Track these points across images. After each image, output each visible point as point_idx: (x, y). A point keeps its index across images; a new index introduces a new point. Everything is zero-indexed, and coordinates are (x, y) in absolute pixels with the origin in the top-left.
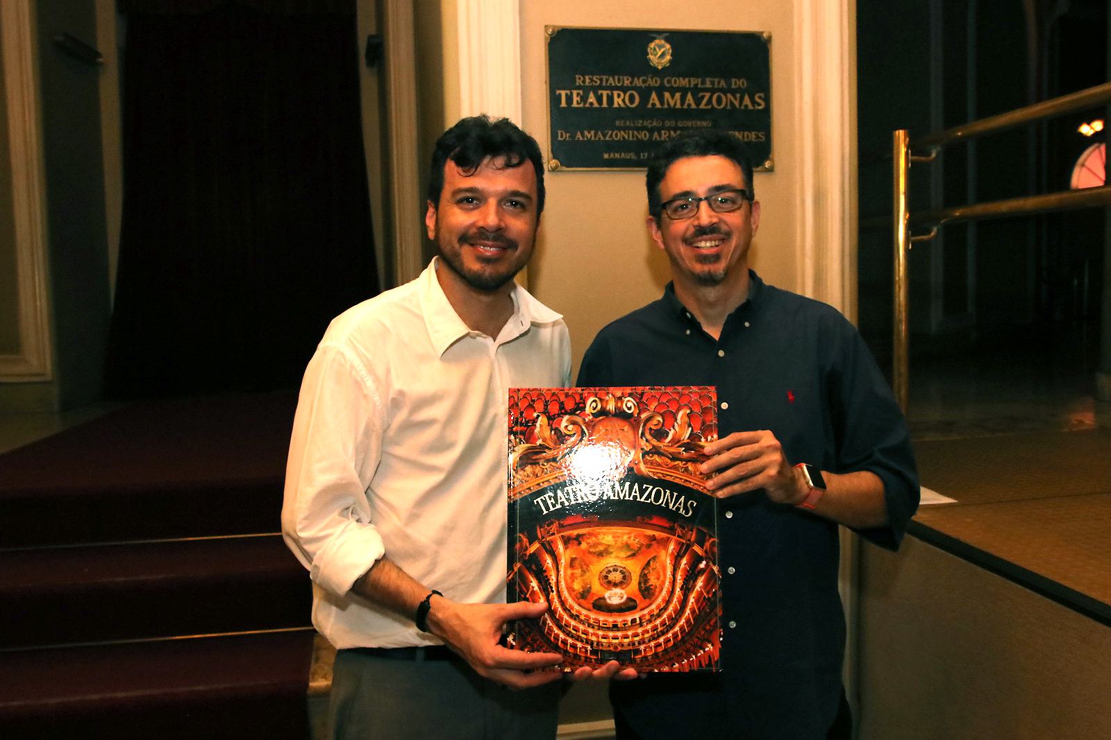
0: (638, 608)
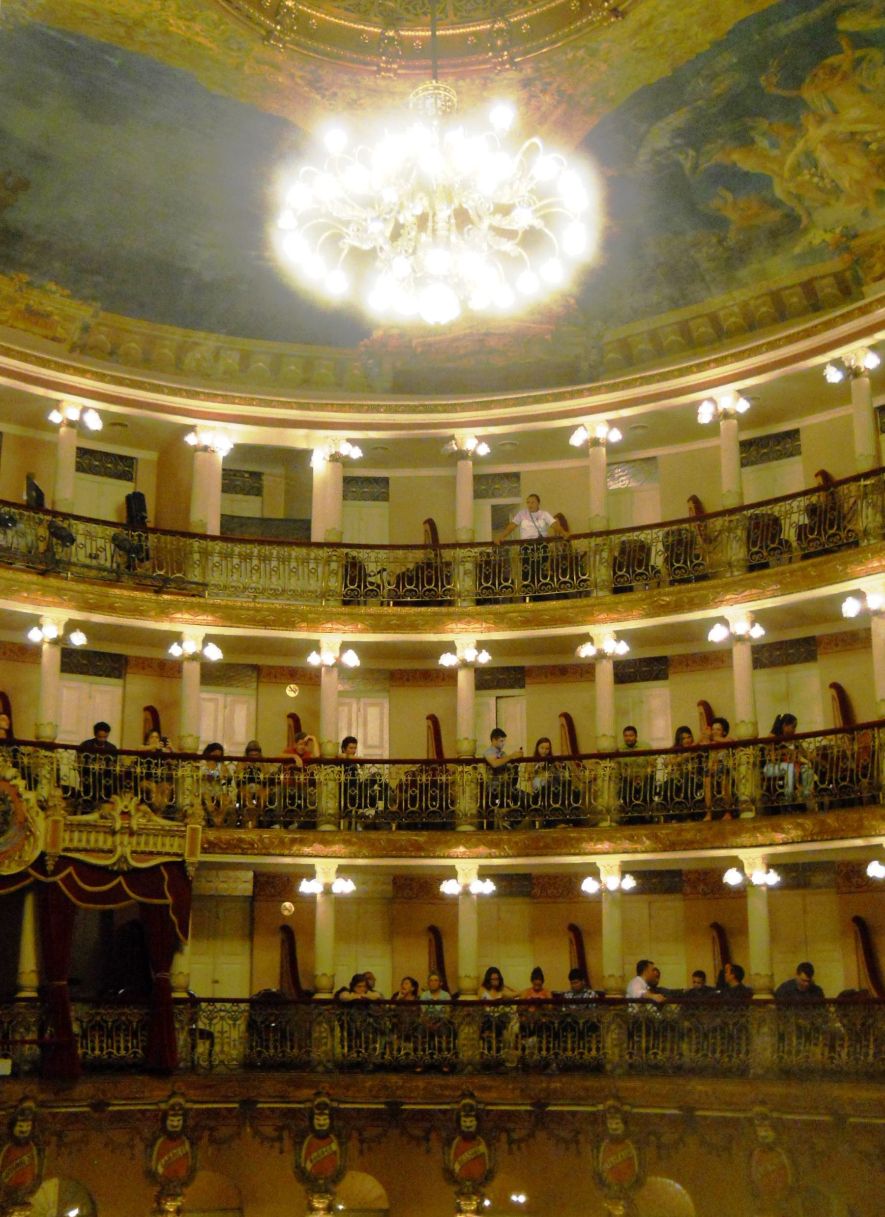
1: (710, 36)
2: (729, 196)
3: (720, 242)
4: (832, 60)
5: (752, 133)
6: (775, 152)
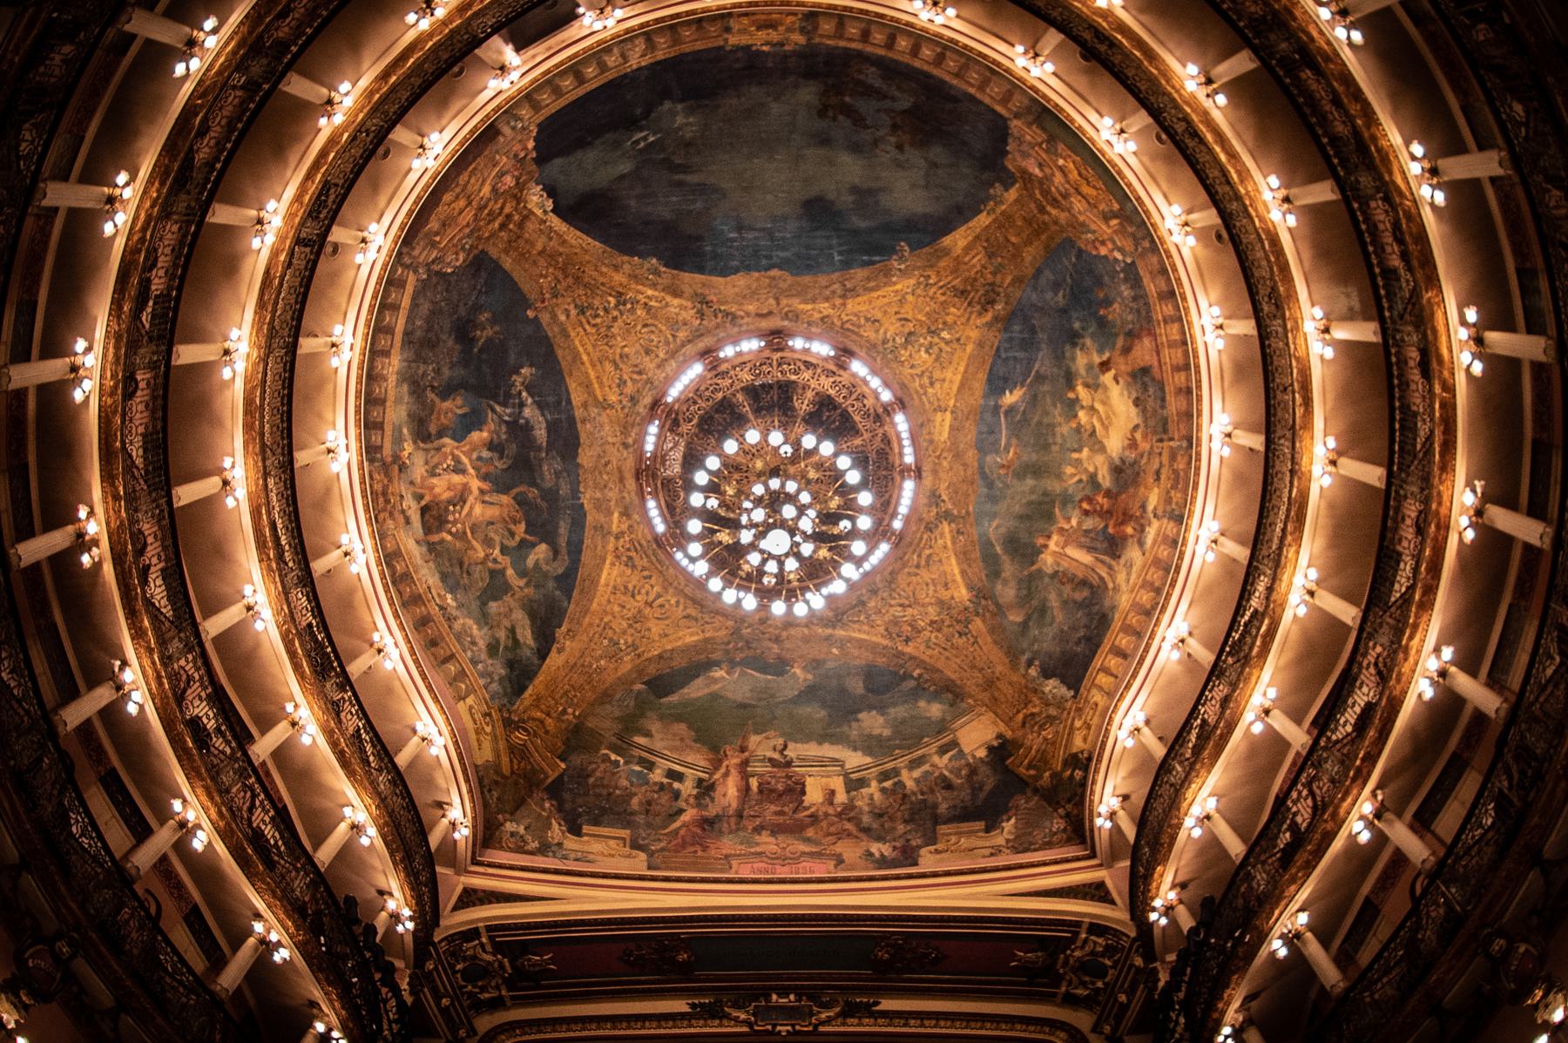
0: (521, 140)
2: (459, 412)
3: (433, 387)
4: (523, 526)
5: (496, 455)
6: (474, 456)
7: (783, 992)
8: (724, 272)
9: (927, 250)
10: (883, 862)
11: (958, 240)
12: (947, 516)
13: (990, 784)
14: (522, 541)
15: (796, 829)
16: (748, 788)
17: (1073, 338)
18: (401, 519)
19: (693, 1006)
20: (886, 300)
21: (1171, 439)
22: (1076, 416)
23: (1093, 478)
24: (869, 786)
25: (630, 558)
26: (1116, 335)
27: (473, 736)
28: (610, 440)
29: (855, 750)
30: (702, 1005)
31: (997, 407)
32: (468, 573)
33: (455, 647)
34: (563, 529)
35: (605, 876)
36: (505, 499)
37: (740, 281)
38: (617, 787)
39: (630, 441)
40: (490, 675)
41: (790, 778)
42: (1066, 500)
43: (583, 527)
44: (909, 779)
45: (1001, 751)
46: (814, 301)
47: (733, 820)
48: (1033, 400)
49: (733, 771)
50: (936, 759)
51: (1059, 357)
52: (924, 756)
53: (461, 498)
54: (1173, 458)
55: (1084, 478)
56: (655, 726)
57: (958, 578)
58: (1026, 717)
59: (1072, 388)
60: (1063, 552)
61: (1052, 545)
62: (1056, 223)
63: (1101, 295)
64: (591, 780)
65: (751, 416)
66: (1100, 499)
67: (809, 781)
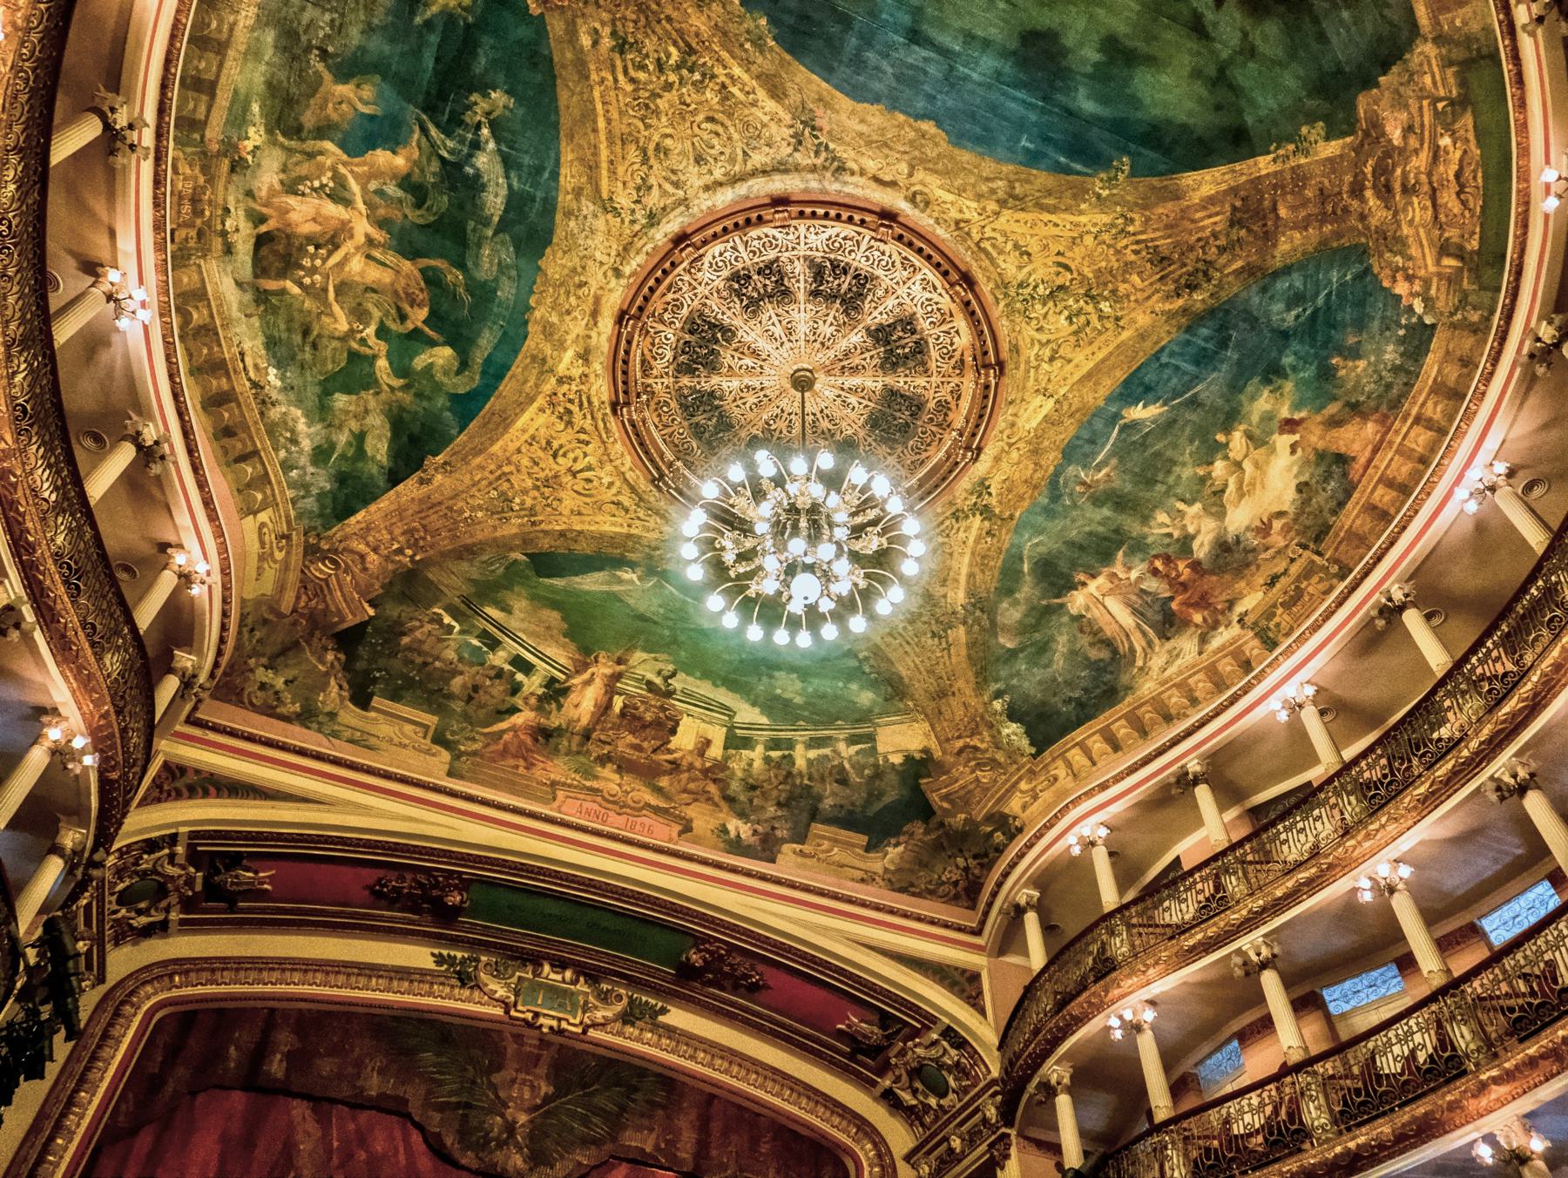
1: (538, 314)
2: (366, 110)
4: (423, 313)
6: (373, 186)
7: (560, 965)
8: (858, 93)
9: (1155, 181)
10: (736, 846)
11: (1205, 183)
12: (986, 512)
13: (891, 796)
14: (416, 331)
15: (648, 773)
16: (609, 706)
17: (1272, 373)
18: (217, 244)
19: (440, 960)
20: (1056, 231)
21: (1319, 554)
22: (1212, 463)
23: (1186, 542)
24: (753, 749)
25: (569, 412)
26: (1335, 399)
27: (253, 562)
28: (598, 255)
29: (754, 704)
30: (451, 961)
31: (1117, 416)
32: (315, 346)
33: (263, 442)
34: (486, 342)
35: (387, 776)
36: (407, 266)
37: (876, 116)
38: (437, 658)
39: (627, 270)
40: (306, 487)
41: (663, 709)
42: (1138, 547)
43: (516, 352)
44: (802, 757)
45: (919, 767)
46: (960, 192)
47: (577, 739)
48: (1167, 426)
49: (598, 682)
50: (842, 746)
51: (1235, 386)
52: (830, 738)
53: (332, 240)
54: (1307, 573)
55: (1176, 534)
56: (520, 604)
57: (963, 579)
58: (967, 746)
59: (1227, 430)
60: (1104, 600)
61: (1093, 586)
62: (1363, 217)
63: (1351, 340)
64: (406, 640)
65: (801, 296)
66: (1181, 566)
67: (685, 721)
